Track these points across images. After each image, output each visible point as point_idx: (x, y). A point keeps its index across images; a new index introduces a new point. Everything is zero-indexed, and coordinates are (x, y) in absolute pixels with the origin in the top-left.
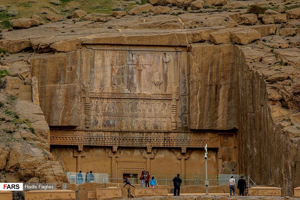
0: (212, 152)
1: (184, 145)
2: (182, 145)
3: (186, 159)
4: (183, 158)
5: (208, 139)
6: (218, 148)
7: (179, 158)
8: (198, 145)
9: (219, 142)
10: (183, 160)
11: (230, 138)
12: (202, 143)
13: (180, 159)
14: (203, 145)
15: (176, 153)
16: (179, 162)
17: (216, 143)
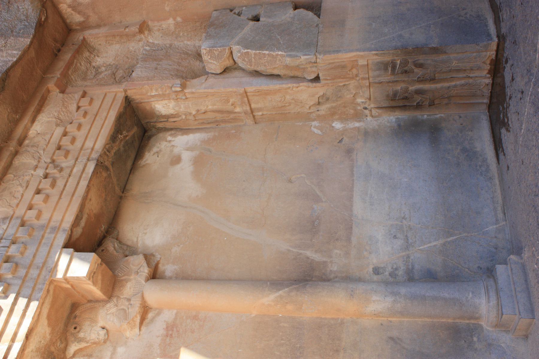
0: (155, 149)
1: (39, 260)
2: (34, 273)
3: (155, 275)
4: (135, 282)
5: (59, 131)
6: (128, 101)
7: (135, 311)
8: (72, 182)
9: (97, 92)
10: (154, 294)
11: (99, 61)
12: (65, 163)
13: (145, 310)
14: (82, 160)
15: (91, 332)
16: (157, 328)
17: (96, 104)
